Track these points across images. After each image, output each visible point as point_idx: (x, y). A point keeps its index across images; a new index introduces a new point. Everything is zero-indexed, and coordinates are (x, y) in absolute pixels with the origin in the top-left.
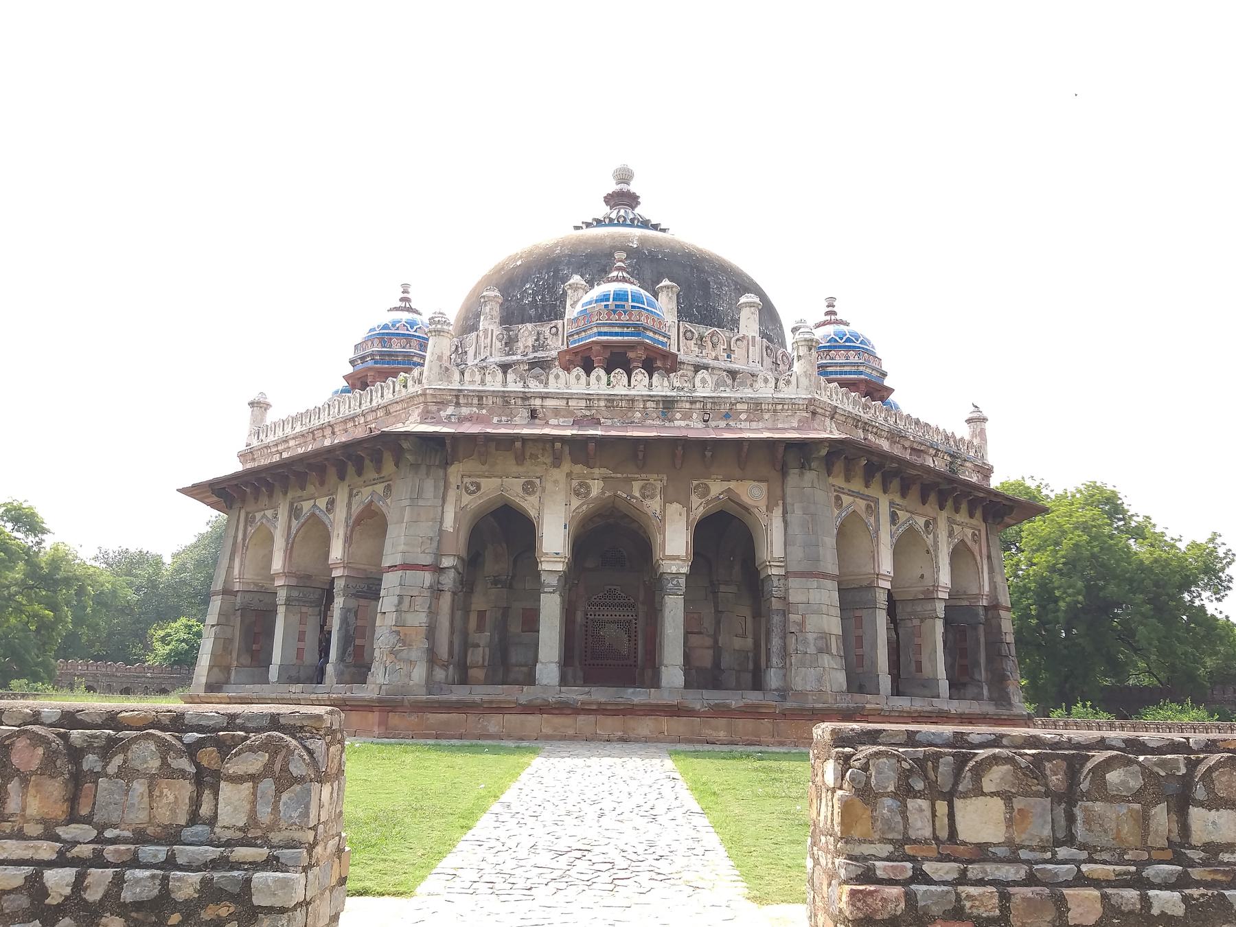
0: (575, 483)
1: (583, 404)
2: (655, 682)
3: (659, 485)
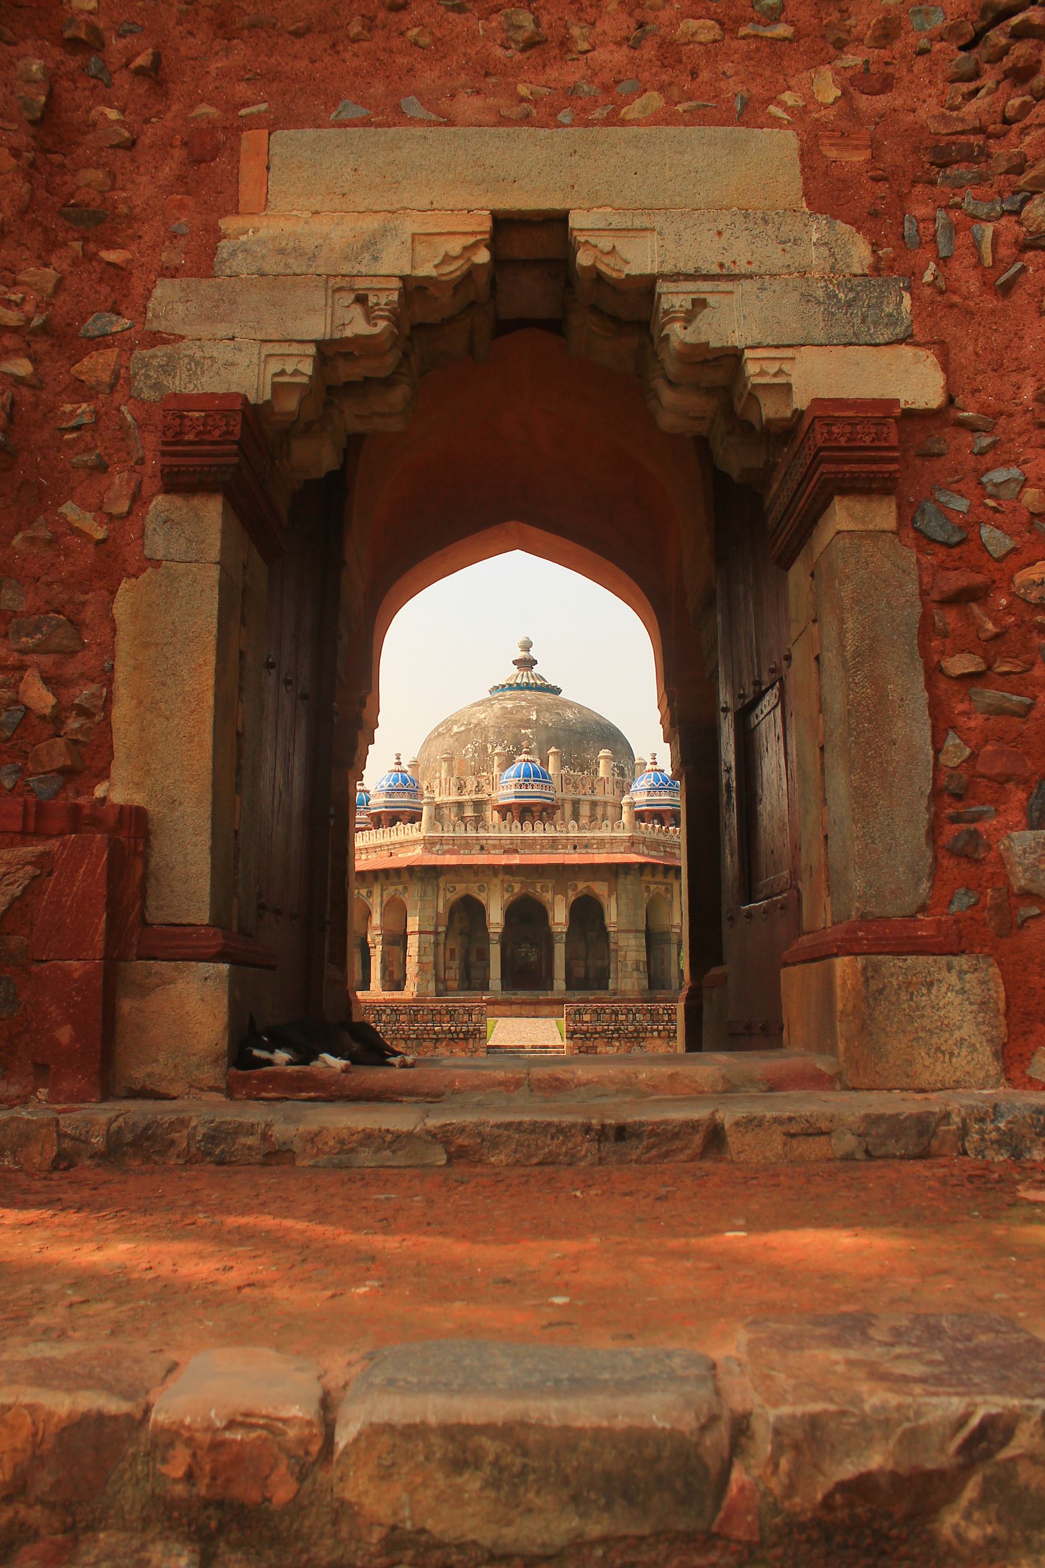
0: (506, 885)
1: (508, 842)
2: (552, 989)
3: (550, 885)
